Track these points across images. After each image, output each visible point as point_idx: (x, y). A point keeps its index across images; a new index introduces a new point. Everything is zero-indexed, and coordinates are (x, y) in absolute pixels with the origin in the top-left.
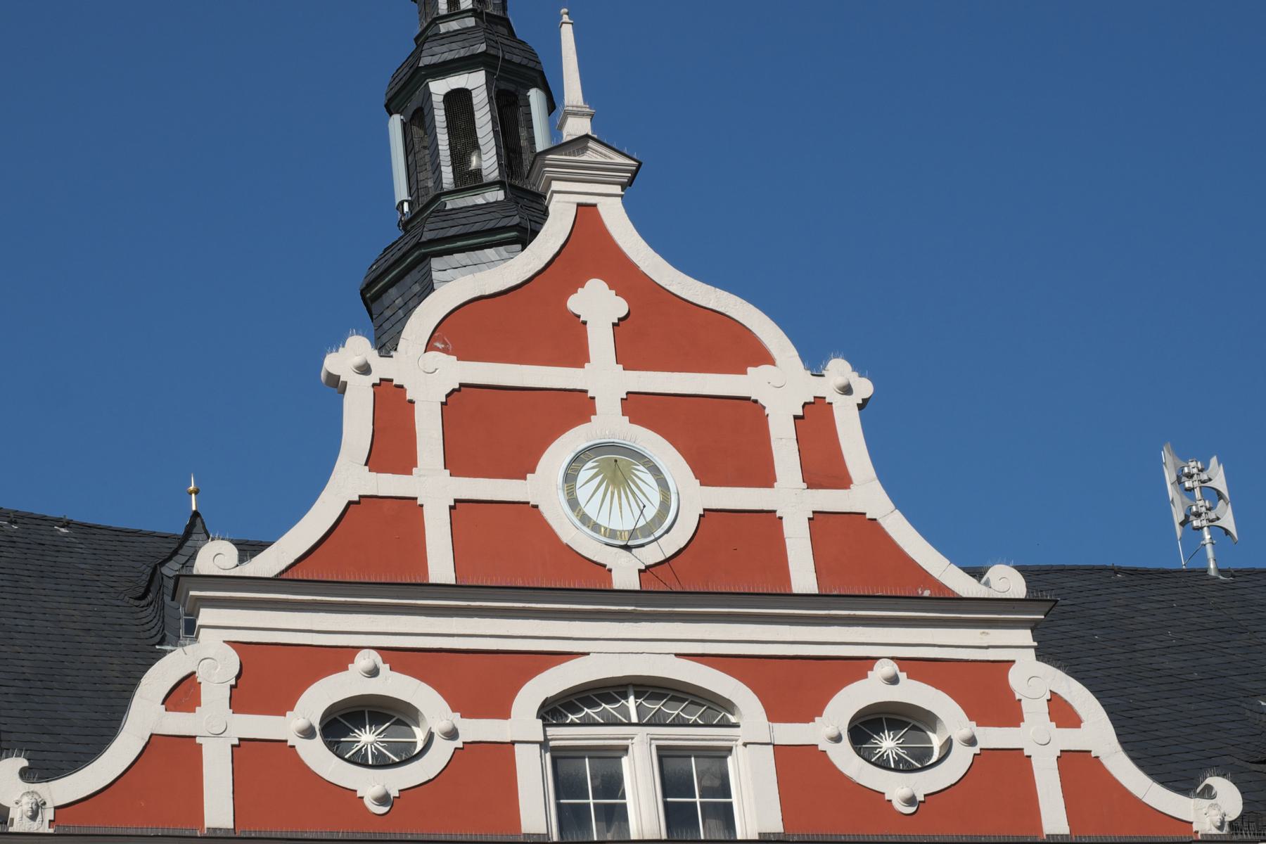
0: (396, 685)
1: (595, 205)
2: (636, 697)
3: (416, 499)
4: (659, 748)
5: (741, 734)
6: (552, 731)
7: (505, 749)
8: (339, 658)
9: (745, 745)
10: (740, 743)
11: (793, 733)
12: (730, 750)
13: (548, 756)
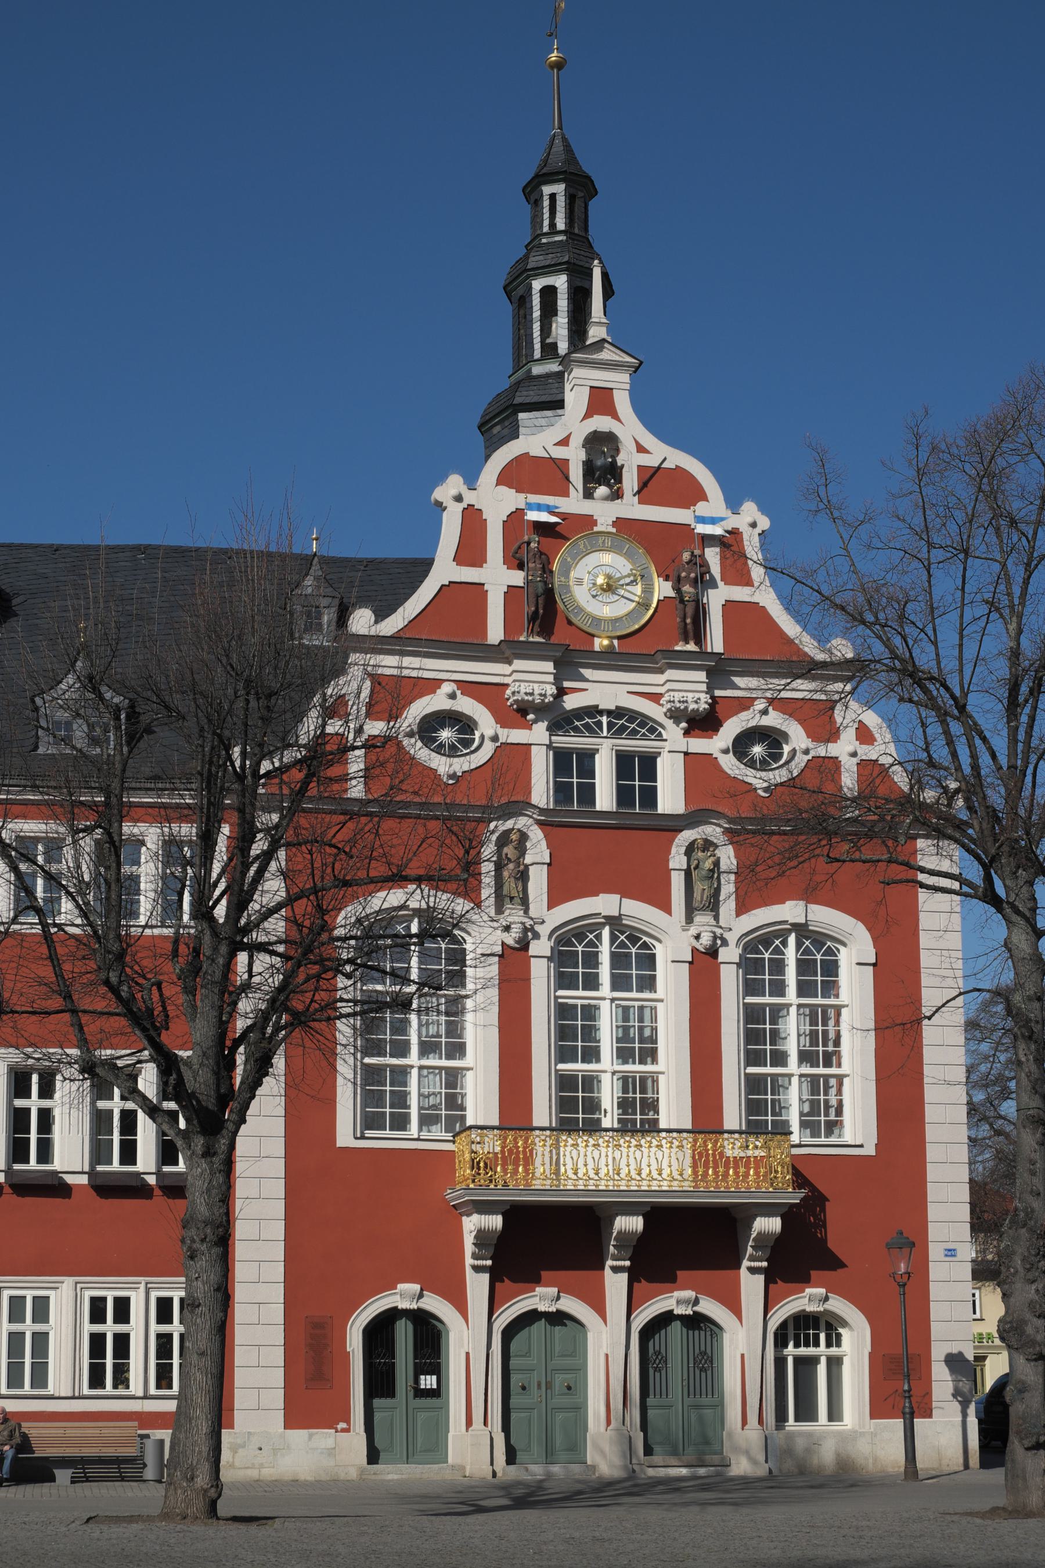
0: (466, 705)
1: (612, 389)
2: (608, 717)
3: (483, 584)
4: (616, 751)
5: (667, 745)
6: (553, 738)
7: (525, 748)
8: (432, 685)
9: (669, 752)
10: (667, 750)
11: (699, 745)
12: (660, 753)
13: (551, 752)
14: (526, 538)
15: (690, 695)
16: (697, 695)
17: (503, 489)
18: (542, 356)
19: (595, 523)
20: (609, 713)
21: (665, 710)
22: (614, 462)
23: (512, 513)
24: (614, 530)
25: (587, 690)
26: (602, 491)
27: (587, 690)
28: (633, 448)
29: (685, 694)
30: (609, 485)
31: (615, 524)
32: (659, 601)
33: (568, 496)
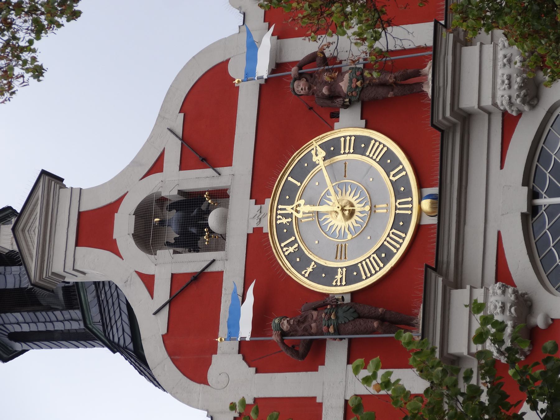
1: (80, 214)
14: (275, 337)
15: (500, 71)
16: (501, 61)
17: (212, 373)
18: (78, 308)
19: (258, 231)
20: (534, 195)
21: (526, 108)
22: (175, 206)
23: (244, 359)
24: (268, 201)
25: (499, 233)
26: (213, 220)
27: (499, 233)
28: (156, 178)
29: (499, 81)
30: (208, 212)
31: (259, 201)
32: (367, 127)
33: (221, 273)
